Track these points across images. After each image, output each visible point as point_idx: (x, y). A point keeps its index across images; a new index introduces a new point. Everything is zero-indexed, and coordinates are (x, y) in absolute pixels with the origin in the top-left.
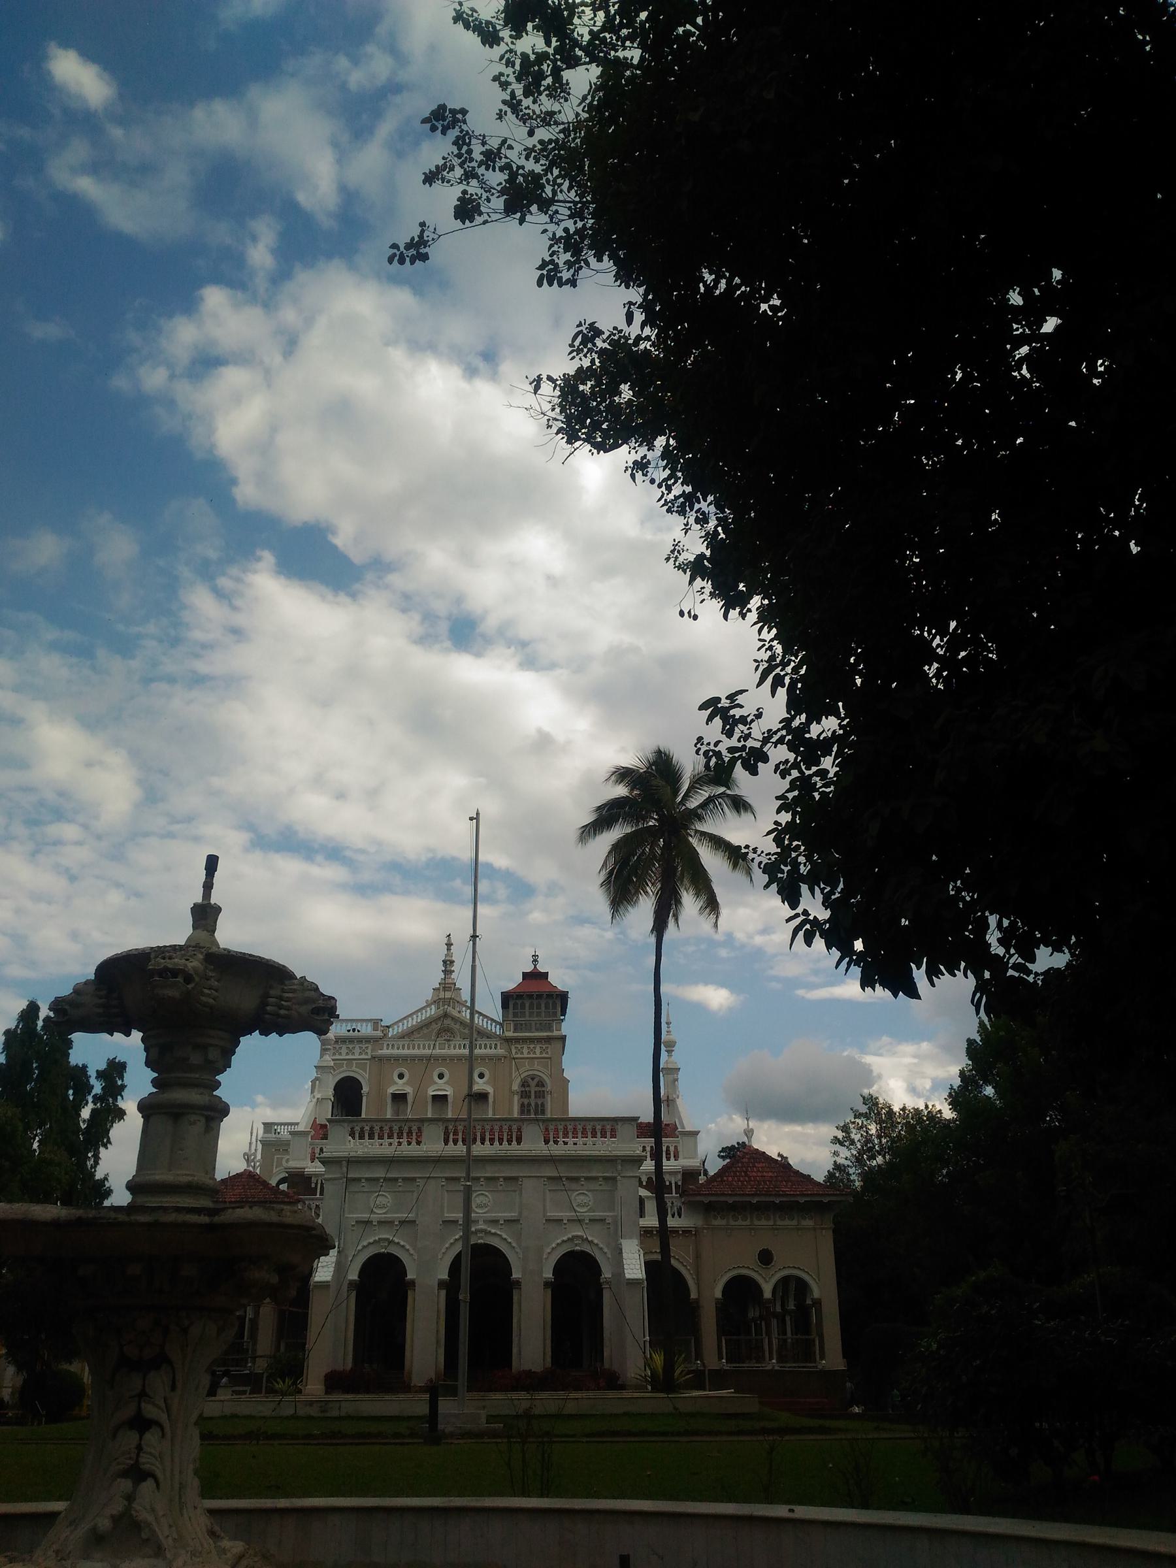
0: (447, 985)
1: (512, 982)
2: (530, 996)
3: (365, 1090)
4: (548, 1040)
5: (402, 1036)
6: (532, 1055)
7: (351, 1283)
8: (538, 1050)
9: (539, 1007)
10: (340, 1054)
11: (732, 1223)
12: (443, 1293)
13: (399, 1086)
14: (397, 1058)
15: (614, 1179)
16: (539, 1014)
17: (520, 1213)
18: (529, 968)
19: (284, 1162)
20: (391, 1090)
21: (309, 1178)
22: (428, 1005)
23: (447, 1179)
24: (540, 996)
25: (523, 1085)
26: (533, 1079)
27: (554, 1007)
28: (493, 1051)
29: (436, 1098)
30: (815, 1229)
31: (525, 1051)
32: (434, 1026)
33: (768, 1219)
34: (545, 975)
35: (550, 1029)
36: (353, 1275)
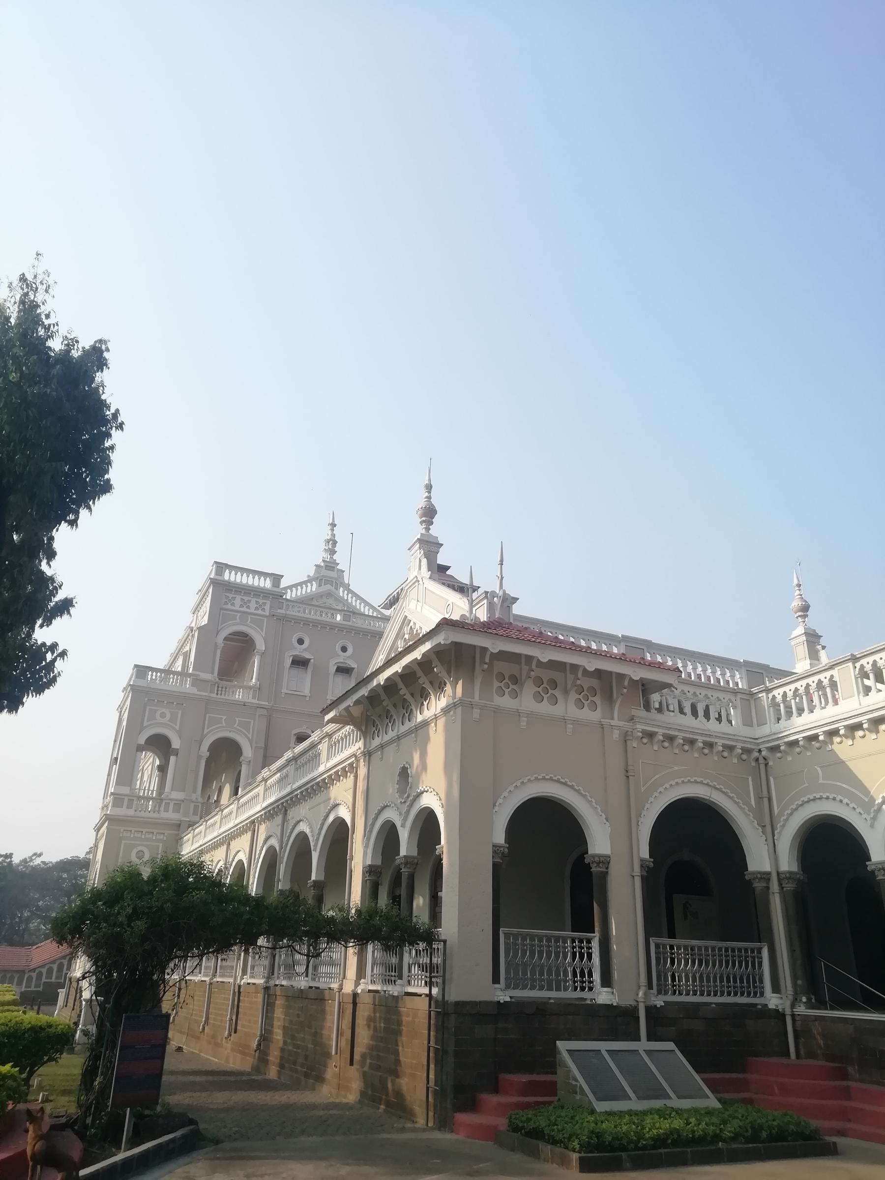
0: (330, 565)
3: (260, 645)
13: (300, 651)
14: (298, 621)
19: (158, 715)
22: (310, 580)
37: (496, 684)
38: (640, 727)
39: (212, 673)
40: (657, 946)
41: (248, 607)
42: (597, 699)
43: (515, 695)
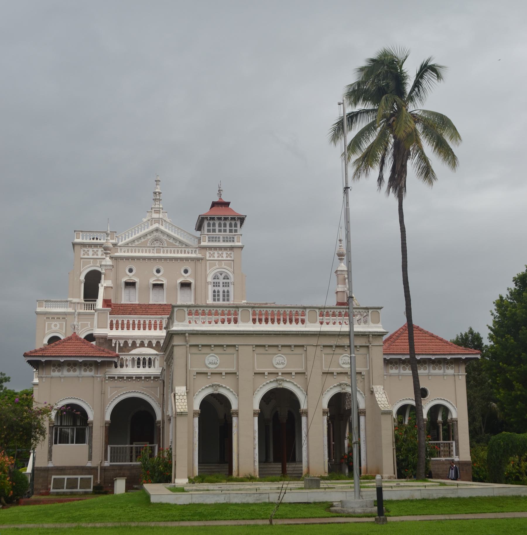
1: (205, 209)
2: (219, 219)
4: (232, 248)
5: (127, 245)
6: (220, 258)
7: (195, 413)
8: (225, 255)
9: (225, 225)
10: (88, 254)
11: (402, 371)
12: (256, 419)
14: (127, 258)
15: (368, 347)
16: (225, 231)
17: (306, 369)
18: (217, 200)
19: (53, 326)
20: (125, 279)
21: (111, 340)
23: (256, 346)
24: (226, 219)
25: (214, 278)
26: (221, 274)
27: (236, 225)
28: (194, 255)
29: (155, 285)
30: (454, 375)
31: (216, 255)
32: (149, 237)
33: (425, 369)
34: (227, 204)
35: (233, 241)
36: (197, 407)
37: (52, 368)
38: (107, 376)
39: (79, 297)
40: (111, 448)
41: (97, 255)
42: (93, 368)
43: (59, 371)
